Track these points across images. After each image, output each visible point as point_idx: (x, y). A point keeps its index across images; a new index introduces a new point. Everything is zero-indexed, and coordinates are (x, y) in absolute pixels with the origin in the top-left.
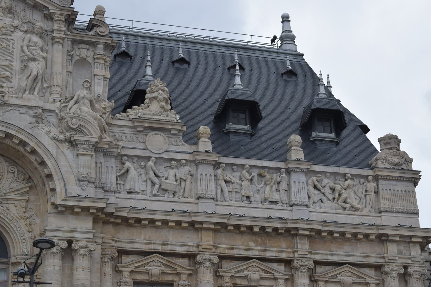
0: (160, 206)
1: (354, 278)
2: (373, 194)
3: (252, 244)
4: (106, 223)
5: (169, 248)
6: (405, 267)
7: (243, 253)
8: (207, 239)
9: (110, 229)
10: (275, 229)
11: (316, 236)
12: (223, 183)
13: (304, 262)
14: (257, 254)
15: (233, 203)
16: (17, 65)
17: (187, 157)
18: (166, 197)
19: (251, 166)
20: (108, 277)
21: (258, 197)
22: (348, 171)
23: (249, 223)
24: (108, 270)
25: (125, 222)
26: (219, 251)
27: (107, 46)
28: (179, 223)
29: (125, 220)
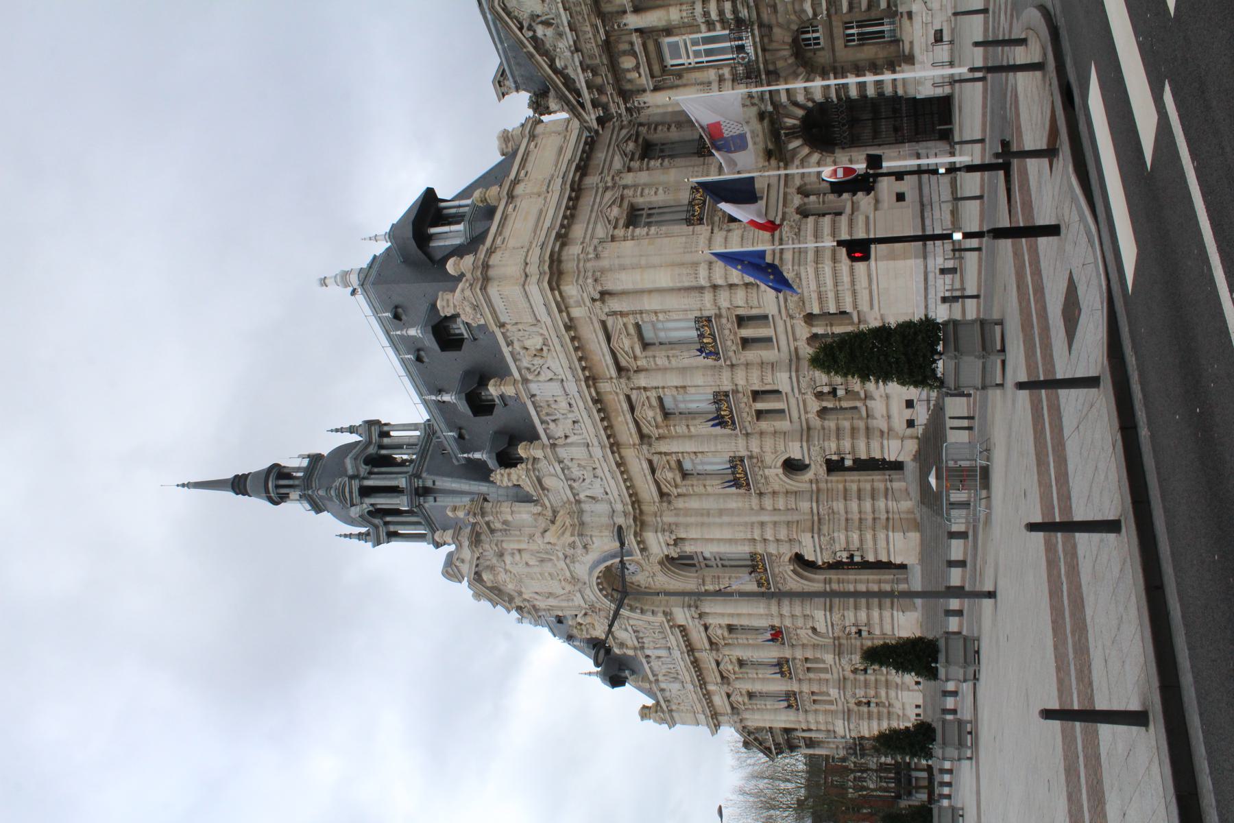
0: (615, 487)
1: (622, 336)
2: (520, 327)
3: (621, 419)
4: (641, 512)
5: (647, 471)
6: (594, 300)
7: (632, 426)
8: (629, 454)
9: (644, 508)
10: (599, 411)
11: (592, 379)
12: (569, 440)
13: (624, 386)
14: (629, 416)
15: (584, 431)
16: (536, 570)
17: (556, 465)
18: (599, 472)
19: (542, 422)
20: (687, 505)
21: (570, 415)
22: (506, 350)
23: (602, 432)
24: (680, 504)
25: (636, 501)
26: (637, 441)
27: (483, 514)
28: (622, 473)
29: (633, 503)
